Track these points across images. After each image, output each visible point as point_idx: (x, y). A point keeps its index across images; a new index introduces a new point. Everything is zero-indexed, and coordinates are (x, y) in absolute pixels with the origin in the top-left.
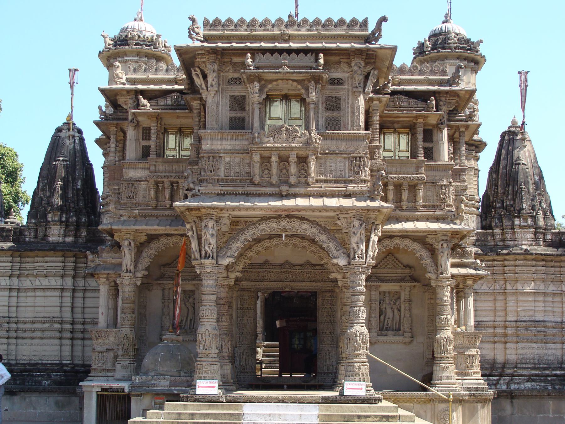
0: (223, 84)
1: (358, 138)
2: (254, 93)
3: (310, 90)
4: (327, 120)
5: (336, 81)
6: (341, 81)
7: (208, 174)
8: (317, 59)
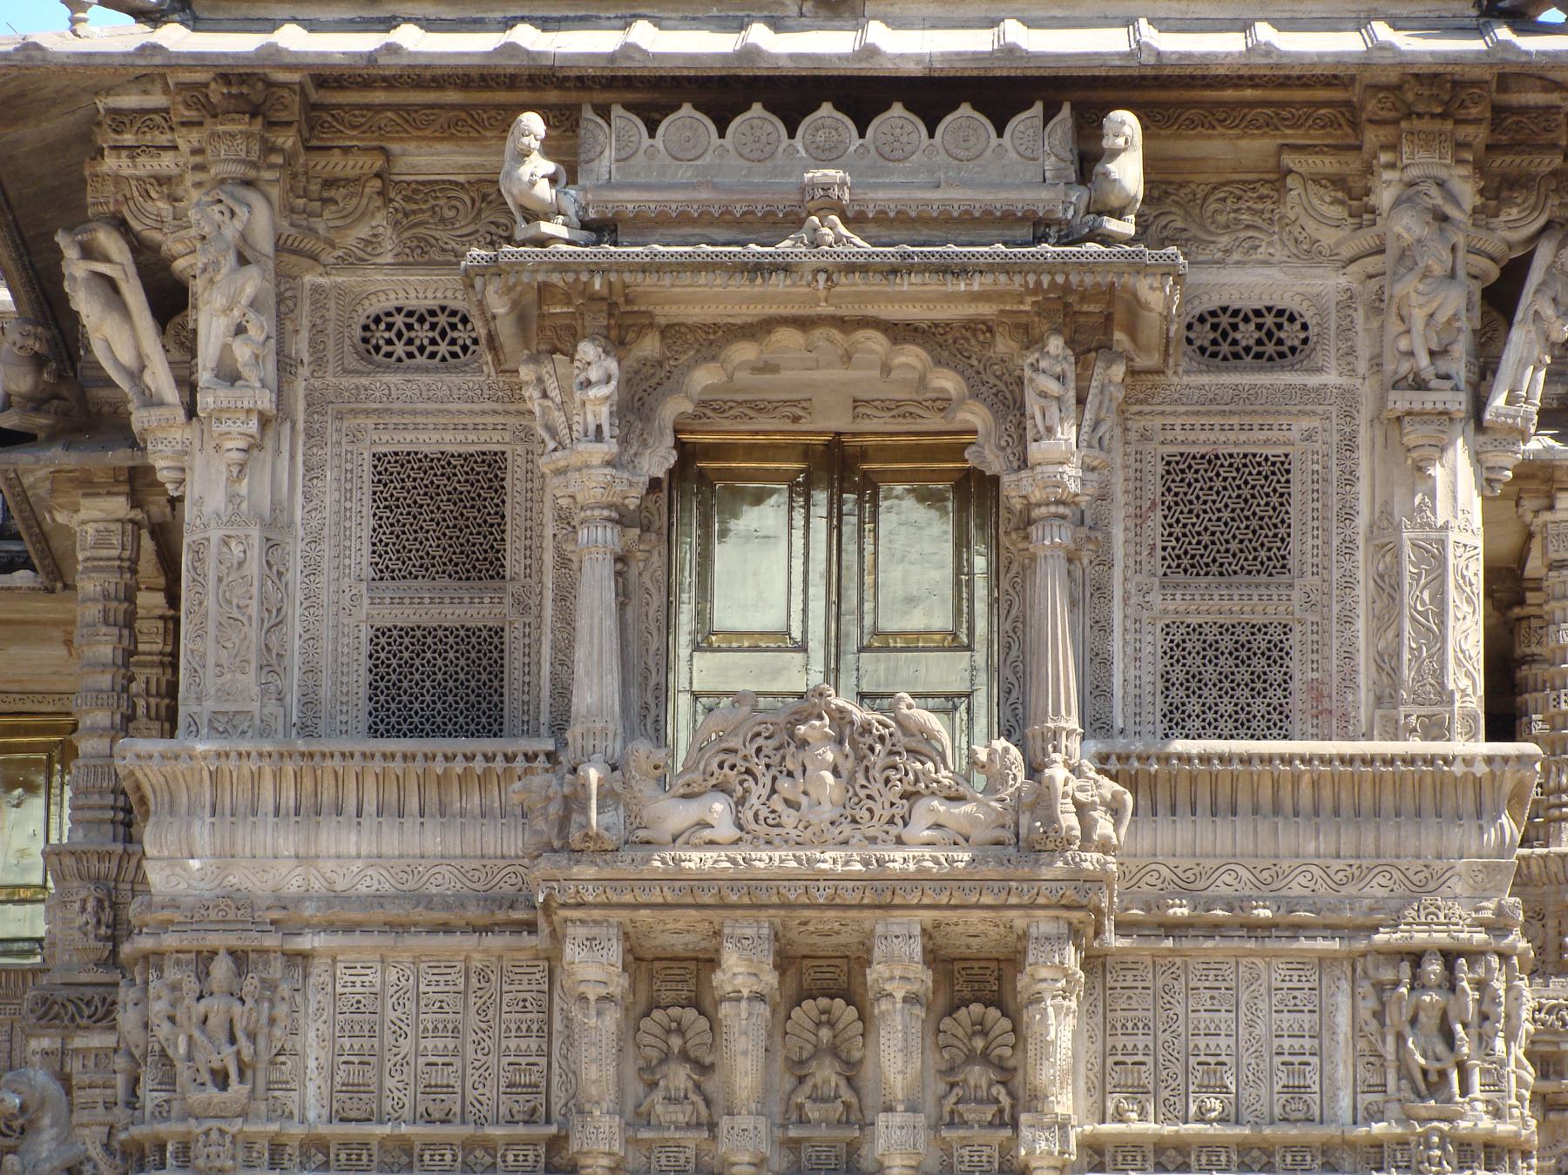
0: (319, 363)
1: (1431, 795)
2: (575, 436)
3: (1033, 405)
4: (1175, 651)
5: (1247, 334)
6: (1291, 334)
7: (196, 1097)
8: (1089, 160)
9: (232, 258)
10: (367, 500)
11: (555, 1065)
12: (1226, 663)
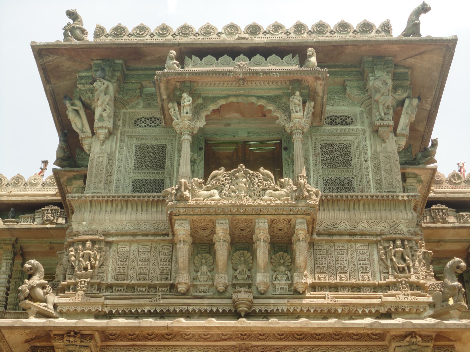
0: (124, 126)
5: (338, 121)
6: (348, 120)
9: (103, 93)
10: (134, 154)
11: (173, 268)
12: (338, 185)
